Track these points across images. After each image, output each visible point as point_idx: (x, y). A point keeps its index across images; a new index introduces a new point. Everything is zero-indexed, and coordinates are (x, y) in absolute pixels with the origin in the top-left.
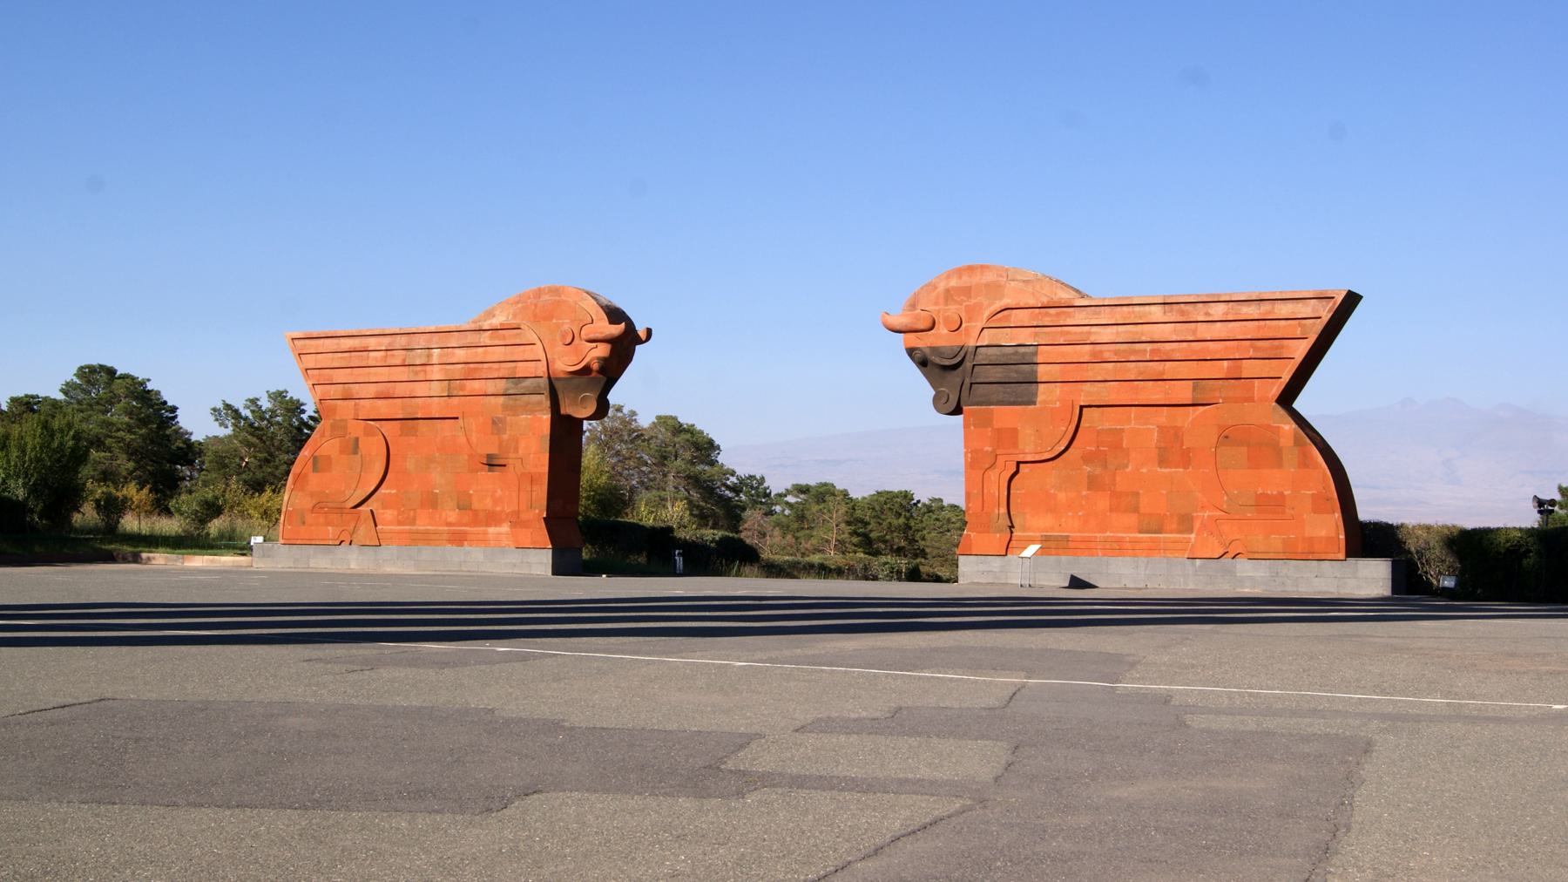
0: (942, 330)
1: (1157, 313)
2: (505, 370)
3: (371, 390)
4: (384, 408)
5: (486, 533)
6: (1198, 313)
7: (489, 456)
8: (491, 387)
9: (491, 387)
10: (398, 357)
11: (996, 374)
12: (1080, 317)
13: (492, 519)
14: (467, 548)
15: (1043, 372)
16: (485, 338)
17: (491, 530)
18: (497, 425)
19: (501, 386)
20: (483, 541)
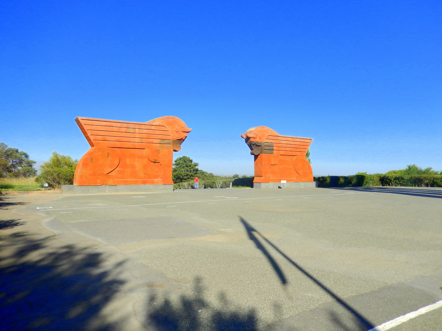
0: (258, 138)
1: (290, 139)
2: (160, 137)
3: (114, 139)
4: (118, 144)
5: (154, 181)
6: (296, 140)
7: (155, 160)
8: (155, 141)
9: (155, 141)
10: (124, 130)
11: (267, 148)
12: (280, 138)
13: (156, 177)
14: (147, 185)
15: (275, 148)
16: (153, 128)
17: (155, 180)
18: (158, 151)
19: (158, 141)
20: (153, 183)
